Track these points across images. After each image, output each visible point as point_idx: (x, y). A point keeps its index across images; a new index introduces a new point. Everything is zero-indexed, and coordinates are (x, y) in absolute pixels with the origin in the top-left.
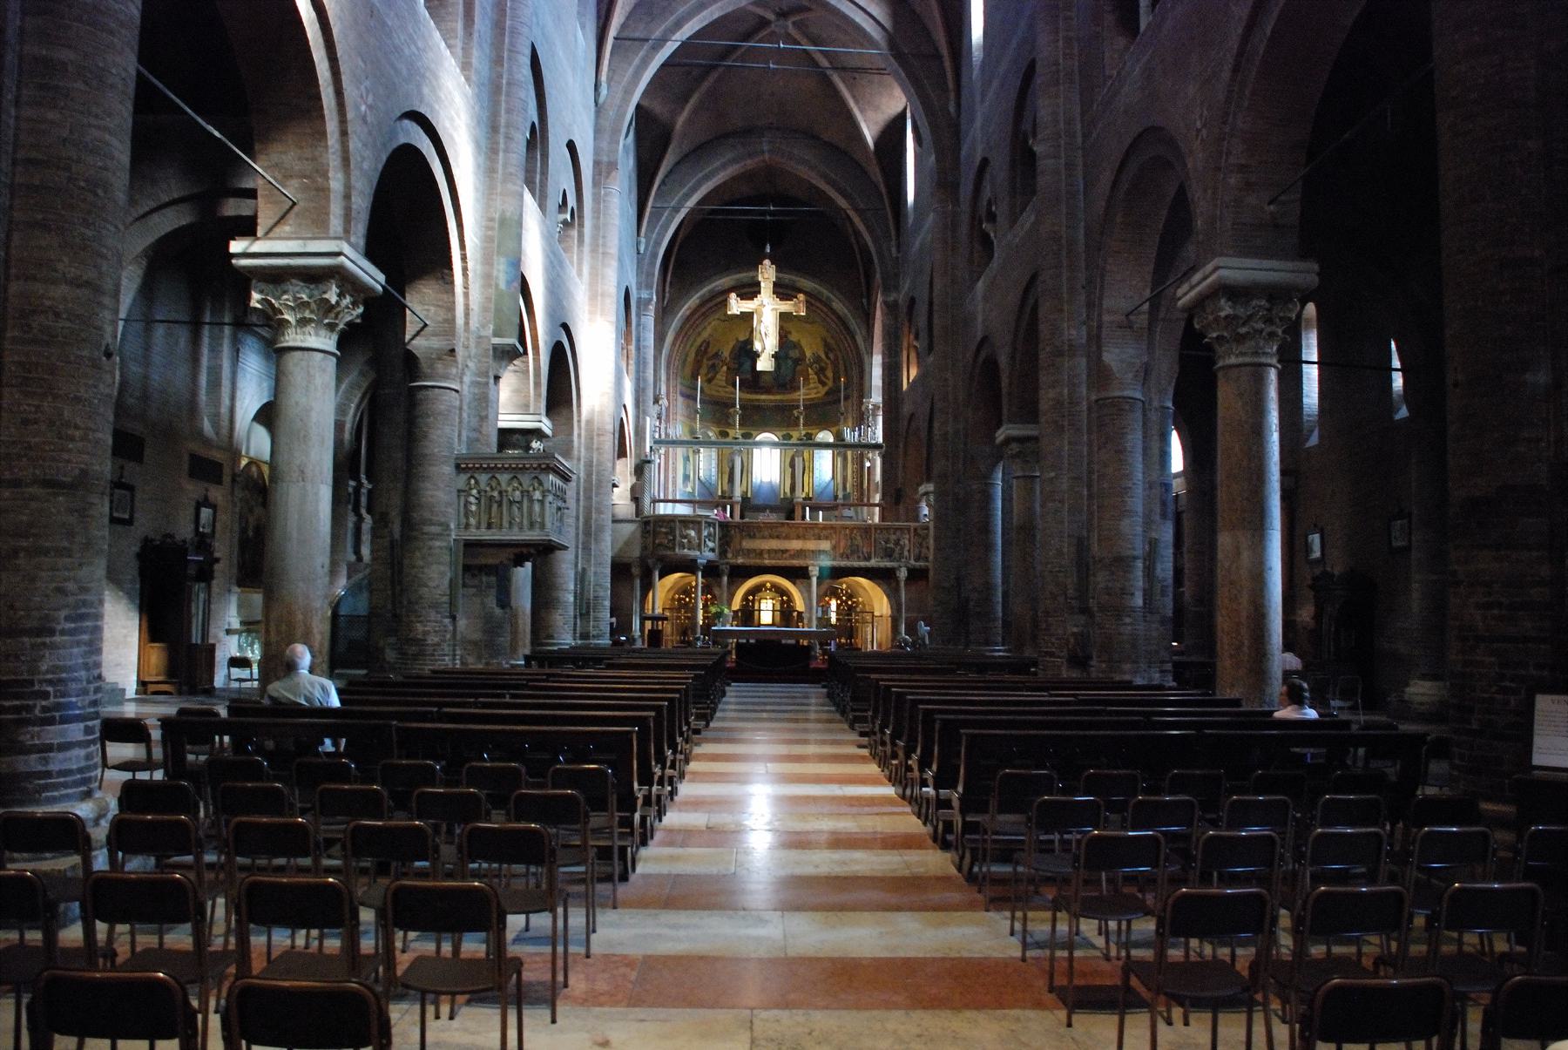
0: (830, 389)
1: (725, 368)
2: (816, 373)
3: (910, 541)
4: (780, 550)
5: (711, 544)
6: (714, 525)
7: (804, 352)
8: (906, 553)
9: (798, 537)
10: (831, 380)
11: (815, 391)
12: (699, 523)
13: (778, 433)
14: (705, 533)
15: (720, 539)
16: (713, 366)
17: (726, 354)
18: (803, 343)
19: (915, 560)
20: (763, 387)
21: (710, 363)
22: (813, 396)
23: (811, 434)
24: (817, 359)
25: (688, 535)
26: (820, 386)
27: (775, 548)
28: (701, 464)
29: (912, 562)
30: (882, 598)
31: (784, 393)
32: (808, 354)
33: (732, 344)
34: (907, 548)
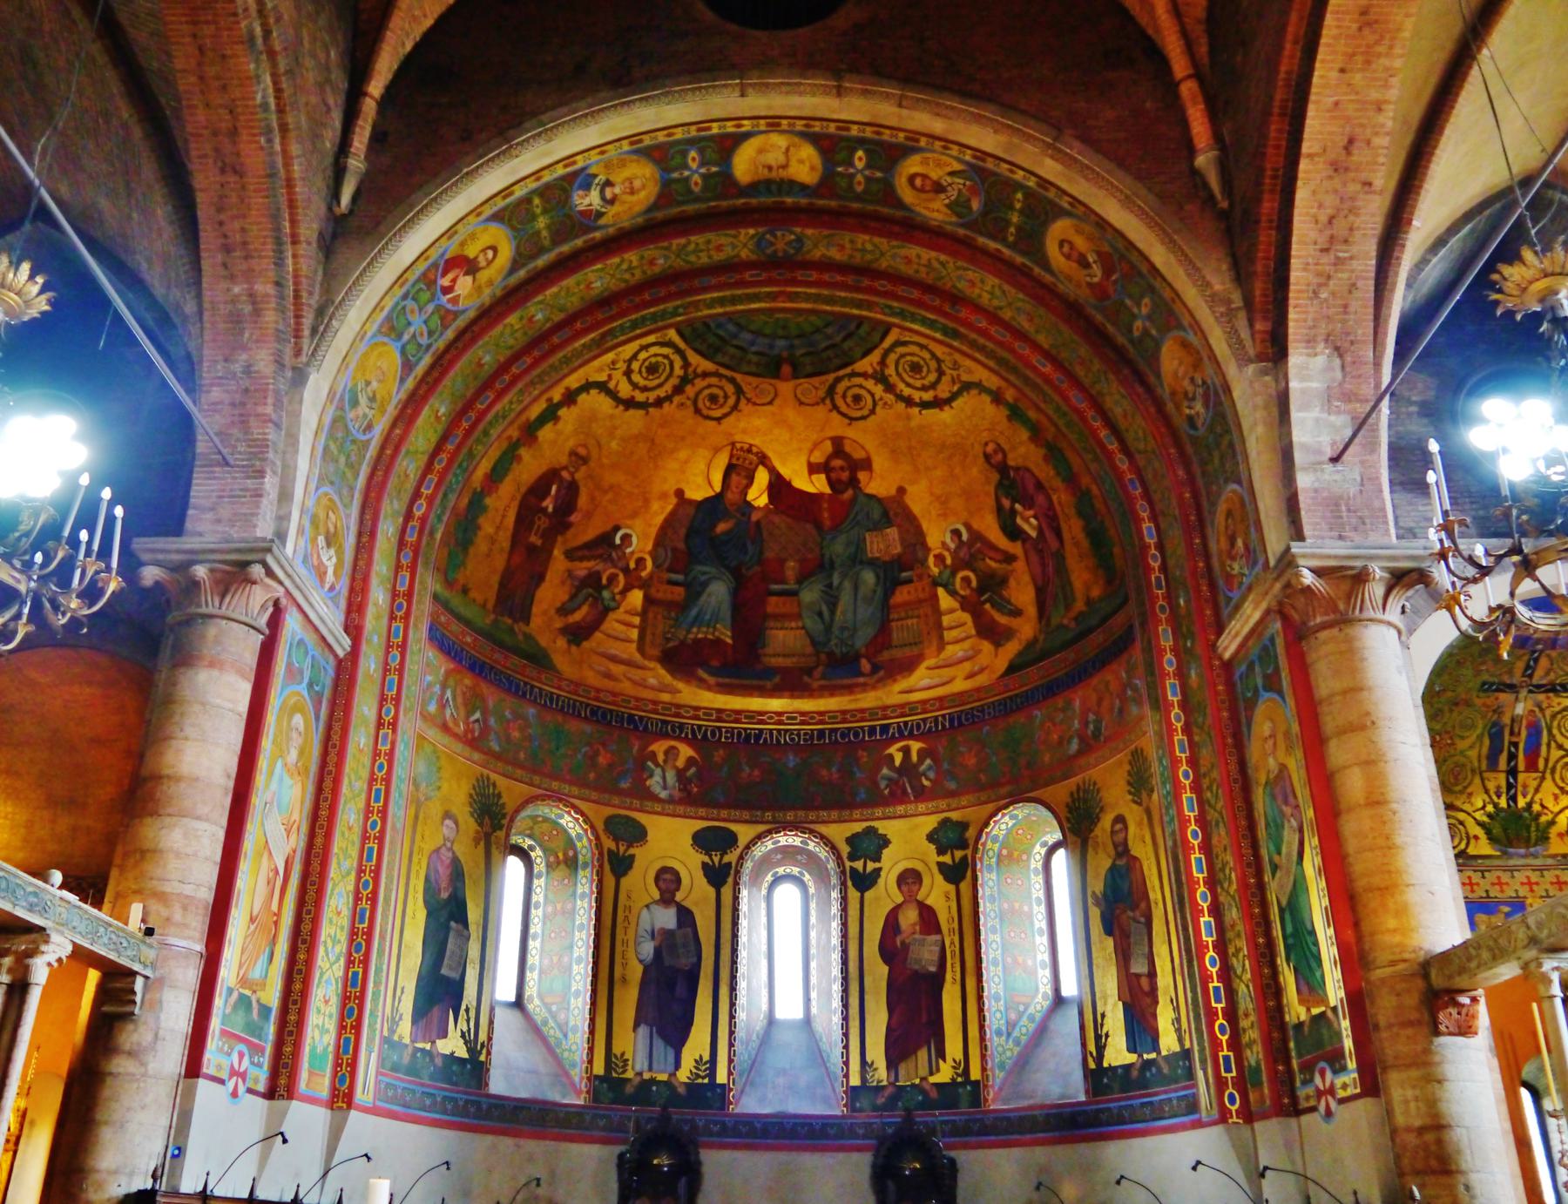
0: (1031, 644)
1: (636, 597)
2: (965, 605)
7: (920, 534)
10: (1031, 611)
11: (967, 666)
13: (840, 832)
16: (593, 580)
17: (640, 540)
18: (918, 501)
20: (770, 672)
21: (582, 568)
22: (960, 685)
23: (963, 826)
24: (971, 549)
26: (986, 646)
31: (850, 689)
32: (937, 536)
33: (659, 512)
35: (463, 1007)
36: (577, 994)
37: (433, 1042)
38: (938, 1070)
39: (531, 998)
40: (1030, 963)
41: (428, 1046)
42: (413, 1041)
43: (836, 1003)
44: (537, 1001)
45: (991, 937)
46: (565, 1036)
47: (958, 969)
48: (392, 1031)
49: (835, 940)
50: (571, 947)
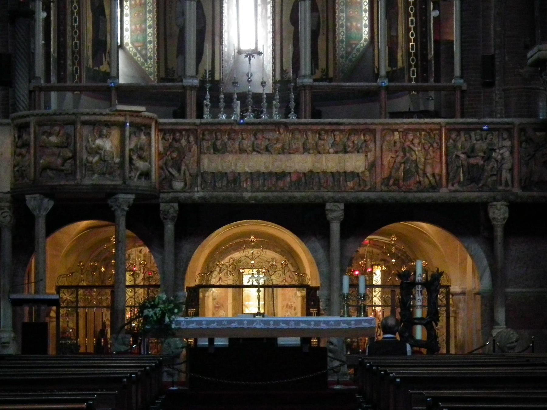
3: (512, 152)
4: (270, 173)
5: (141, 164)
6: (150, 127)
8: (505, 175)
9: (306, 150)
12: (122, 126)
14: (131, 144)
15: (160, 155)
19: (524, 188)
25: (99, 148)
27: (263, 170)
28: (127, 20)
29: (517, 190)
30: (463, 262)
34: (507, 166)
35: (107, 51)
36: (150, 42)
37: (99, 67)
38: (315, 73)
39: (127, 44)
40: (359, 25)
41: (97, 68)
42: (93, 67)
43: (270, 43)
44: (130, 45)
45: (341, 14)
46: (146, 61)
47: (325, 28)
48: (88, 64)
49: (269, 14)
50: (145, 21)
